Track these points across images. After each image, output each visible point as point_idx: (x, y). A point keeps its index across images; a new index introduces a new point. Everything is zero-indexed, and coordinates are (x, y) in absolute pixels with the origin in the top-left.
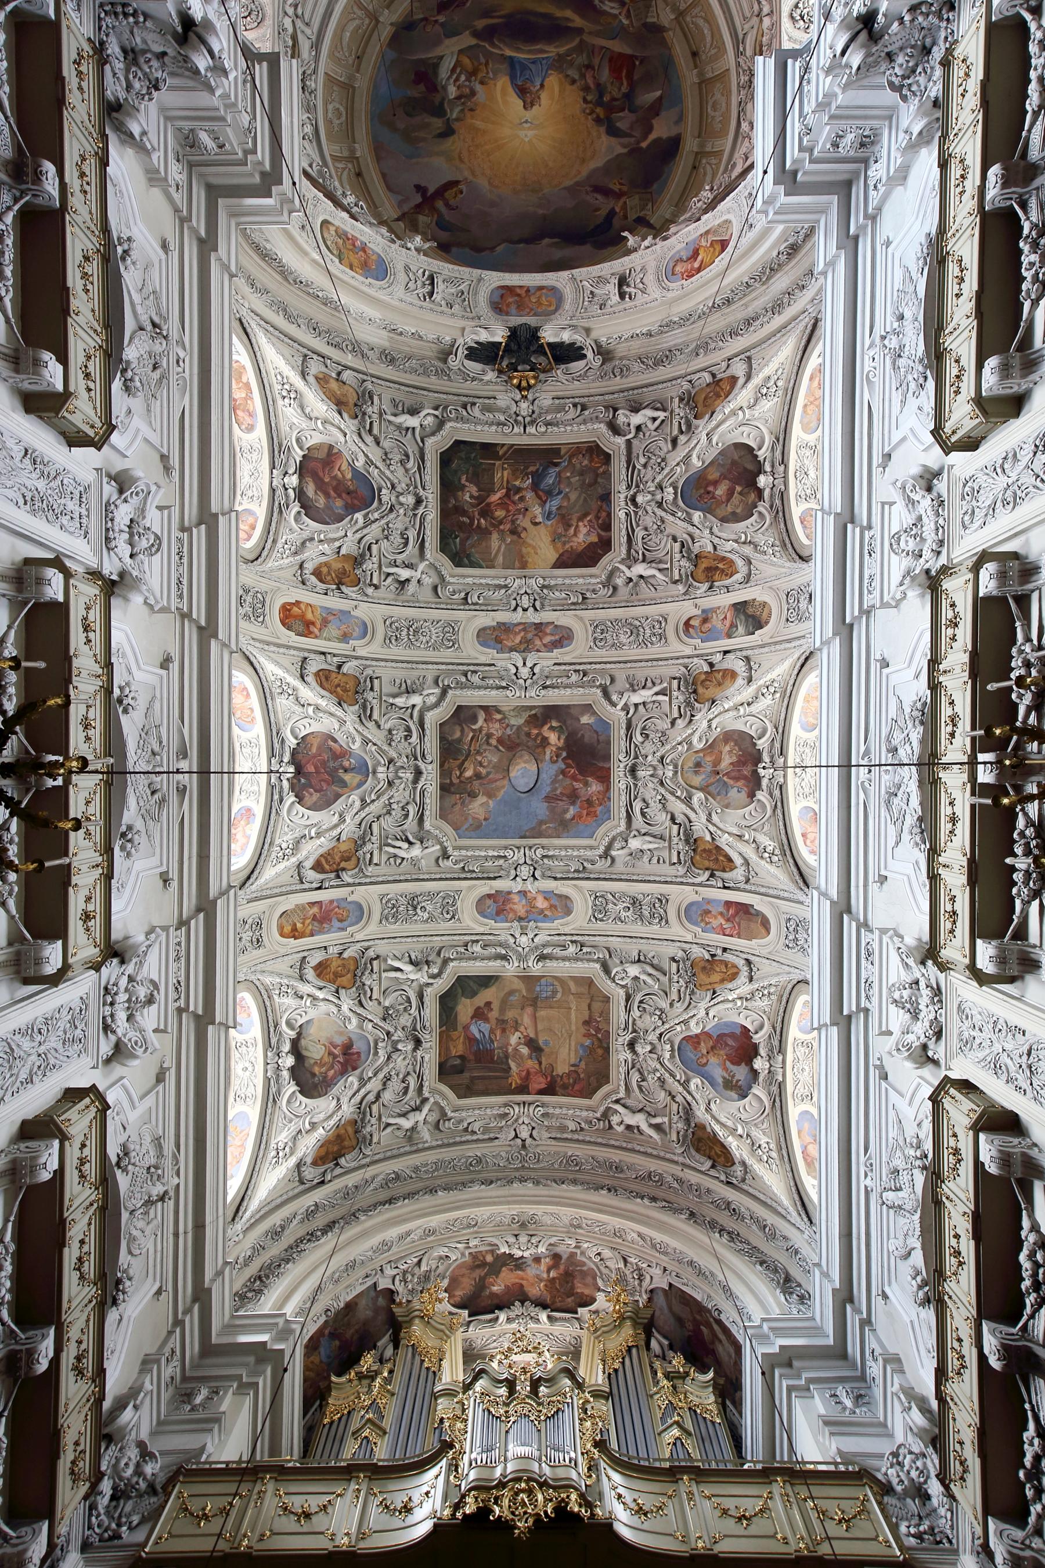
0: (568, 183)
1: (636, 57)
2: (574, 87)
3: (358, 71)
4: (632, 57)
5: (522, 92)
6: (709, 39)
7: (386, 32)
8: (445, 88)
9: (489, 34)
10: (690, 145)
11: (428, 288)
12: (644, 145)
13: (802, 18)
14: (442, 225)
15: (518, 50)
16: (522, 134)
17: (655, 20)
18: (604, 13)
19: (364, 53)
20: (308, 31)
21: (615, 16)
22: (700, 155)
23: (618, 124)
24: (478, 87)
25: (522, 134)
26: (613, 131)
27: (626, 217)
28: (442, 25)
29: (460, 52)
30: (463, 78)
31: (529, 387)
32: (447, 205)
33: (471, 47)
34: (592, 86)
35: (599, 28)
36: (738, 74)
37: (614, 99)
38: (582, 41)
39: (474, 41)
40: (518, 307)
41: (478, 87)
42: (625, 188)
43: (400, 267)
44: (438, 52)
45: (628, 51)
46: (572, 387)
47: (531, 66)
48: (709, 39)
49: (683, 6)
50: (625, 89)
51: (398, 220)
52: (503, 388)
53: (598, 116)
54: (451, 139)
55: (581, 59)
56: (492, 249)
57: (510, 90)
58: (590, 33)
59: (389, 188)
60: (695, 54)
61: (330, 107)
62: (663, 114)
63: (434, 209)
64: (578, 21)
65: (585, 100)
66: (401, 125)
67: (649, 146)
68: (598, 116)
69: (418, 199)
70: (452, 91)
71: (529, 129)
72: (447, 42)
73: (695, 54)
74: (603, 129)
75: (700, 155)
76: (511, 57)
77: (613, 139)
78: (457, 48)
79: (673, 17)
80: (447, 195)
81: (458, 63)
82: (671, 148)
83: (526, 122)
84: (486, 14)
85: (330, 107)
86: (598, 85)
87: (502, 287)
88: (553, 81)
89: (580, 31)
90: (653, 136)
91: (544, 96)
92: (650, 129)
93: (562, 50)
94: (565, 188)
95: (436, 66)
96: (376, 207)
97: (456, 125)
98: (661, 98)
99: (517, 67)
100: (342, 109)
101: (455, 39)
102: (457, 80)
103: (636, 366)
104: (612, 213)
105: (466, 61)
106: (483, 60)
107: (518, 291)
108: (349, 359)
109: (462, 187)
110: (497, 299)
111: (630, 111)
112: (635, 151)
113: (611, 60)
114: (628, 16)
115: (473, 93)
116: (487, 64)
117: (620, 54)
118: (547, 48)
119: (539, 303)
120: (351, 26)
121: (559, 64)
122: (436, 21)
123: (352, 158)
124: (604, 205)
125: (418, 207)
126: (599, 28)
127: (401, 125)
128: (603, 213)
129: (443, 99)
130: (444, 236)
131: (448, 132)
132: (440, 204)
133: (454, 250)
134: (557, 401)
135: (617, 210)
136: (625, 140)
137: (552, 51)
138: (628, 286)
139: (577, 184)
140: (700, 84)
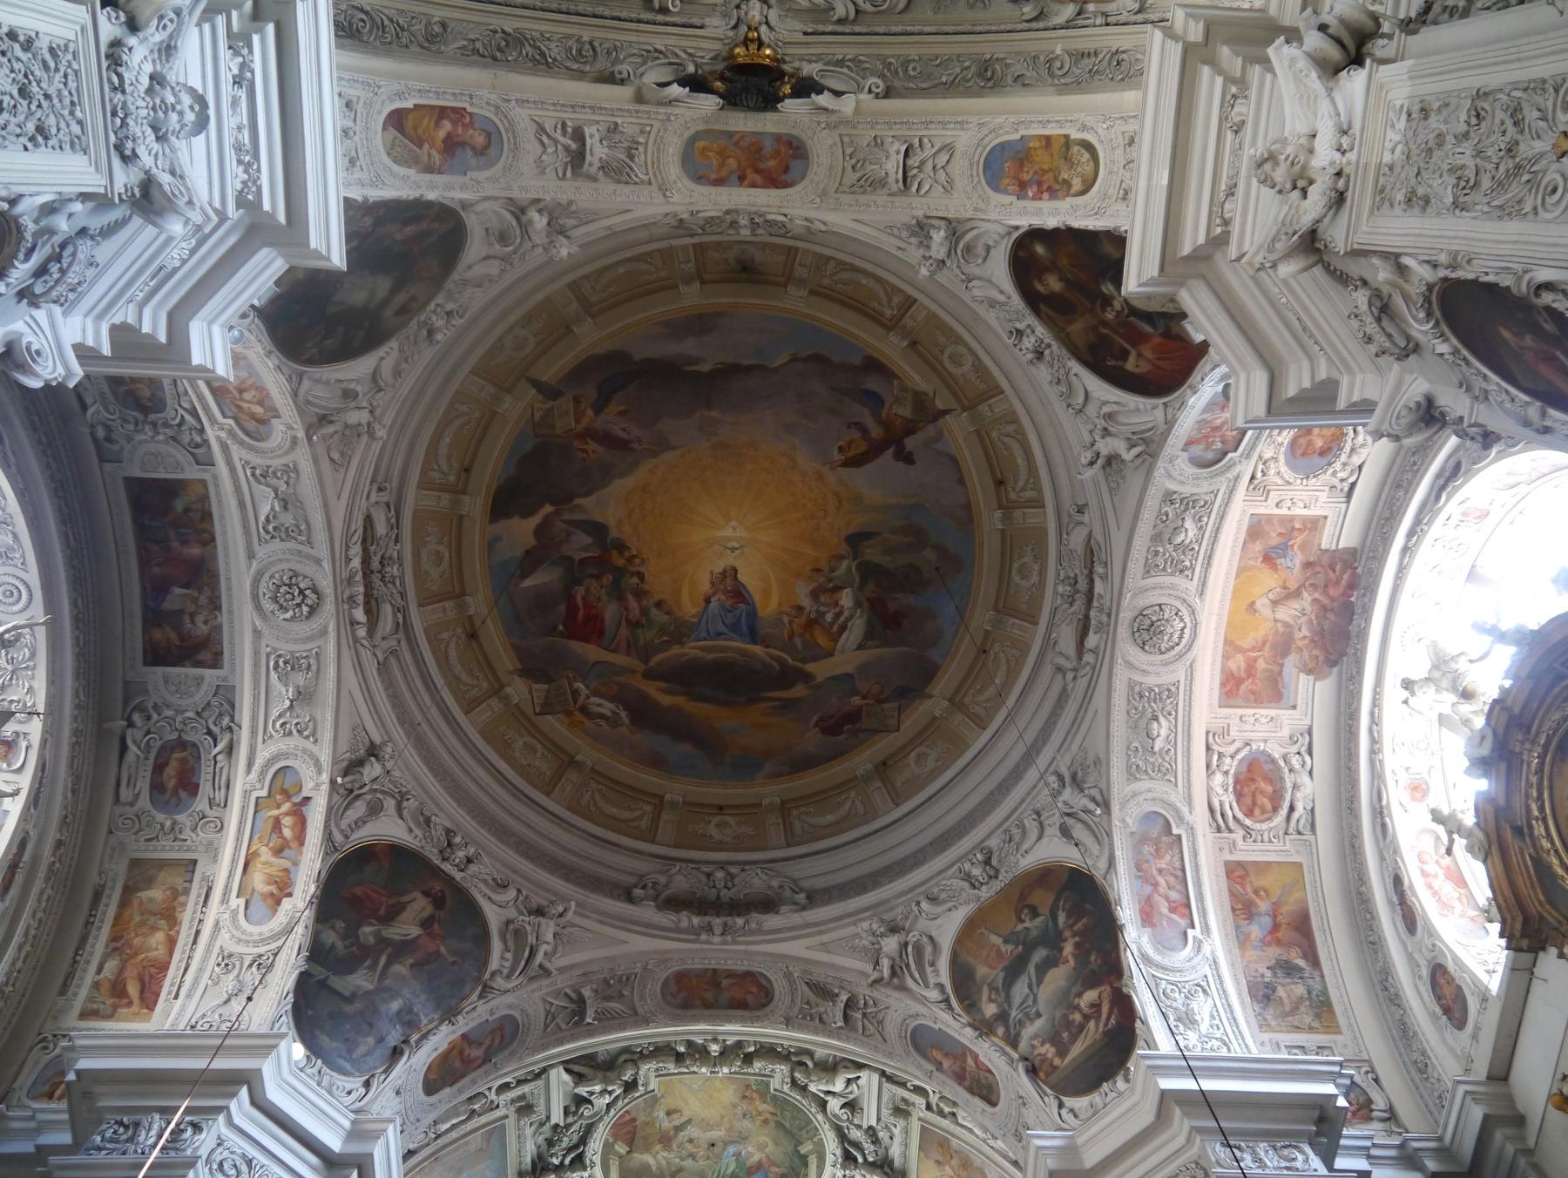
0: (669, 457)
1: (562, 635)
2: (657, 597)
3: (987, 633)
4: (570, 637)
5: (739, 594)
6: (453, 653)
7: (942, 686)
8: (858, 604)
9: (788, 676)
10: (476, 505)
11: (910, 162)
12: (548, 509)
13: (301, 592)
14: (874, 400)
15: (743, 652)
16: (741, 533)
17: (535, 686)
18: (612, 699)
19: (976, 659)
20: (1061, 661)
21: (596, 693)
22: (458, 490)
23: (588, 540)
24: (806, 602)
25: (741, 533)
26: (598, 530)
27: (576, 400)
28: (855, 692)
29: (830, 654)
30: (829, 617)
31: (746, 42)
32: (865, 431)
33: (815, 659)
34: (630, 597)
35: (619, 679)
36: (402, 578)
37: (597, 577)
38: (646, 662)
39: (809, 667)
40: (760, 149)
41: (806, 602)
42: (577, 444)
43: (960, 184)
44: (865, 655)
45: (578, 647)
46: (672, 41)
47: (723, 629)
48: (453, 653)
49: (495, 703)
50: (580, 592)
51: (945, 412)
52: (791, 50)
53: (621, 553)
54: (852, 530)
55: (646, 636)
56: (795, 359)
57: (757, 598)
58: (634, 672)
59: (954, 461)
60: (473, 636)
61: (1035, 579)
62: (519, 553)
63: (886, 425)
64: (653, 689)
65: (641, 576)
66: (929, 554)
67: (541, 506)
68: (621, 553)
69: (910, 443)
70: (846, 599)
71: (729, 539)
72: (850, 668)
73: (473, 636)
74: (614, 533)
75: (458, 490)
76: (755, 642)
77: (600, 519)
78: (837, 658)
79: (509, 690)
80: (862, 447)
81: (835, 638)
82: (506, 503)
83: (733, 550)
84: (788, 705)
85: (1035, 579)
86: (621, 598)
87: (786, 185)
88: (689, 608)
89: (649, 675)
90: (535, 521)
91: (705, 585)
92: (539, 531)
93: (676, 650)
94: (674, 448)
95: (869, 635)
96: (978, 432)
97: (844, 549)
98: (524, 576)
99: (745, 629)
100: (1017, 579)
101: (837, 672)
102: (838, 615)
103: (554, 50)
104: (599, 408)
105: (822, 640)
106: (798, 641)
107: (758, 178)
108: (1059, 45)
109: (837, 457)
110: (796, 165)
111: (570, 559)
112: (563, 499)
113: (601, 633)
114: (575, 693)
115: (814, 594)
116: (791, 636)
117: (586, 640)
118: (700, 654)
119: (723, 155)
120: (991, 691)
121: (680, 632)
122: (864, 697)
123: (1007, 507)
124: (612, 421)
125: (911, 431)
126: (619, 679)
127: (929, 554)
128: (614, 407)
129: (861, 588)
130: (873, 383)
131: (856, 540)
132: (876, 432)
133: (857, 361)
134: (696, 21)
135: (590, 412)
136: (577, 516)
137: (691, 649)
138: (567, 148)
139: (655, 454)
140: (463, 594)
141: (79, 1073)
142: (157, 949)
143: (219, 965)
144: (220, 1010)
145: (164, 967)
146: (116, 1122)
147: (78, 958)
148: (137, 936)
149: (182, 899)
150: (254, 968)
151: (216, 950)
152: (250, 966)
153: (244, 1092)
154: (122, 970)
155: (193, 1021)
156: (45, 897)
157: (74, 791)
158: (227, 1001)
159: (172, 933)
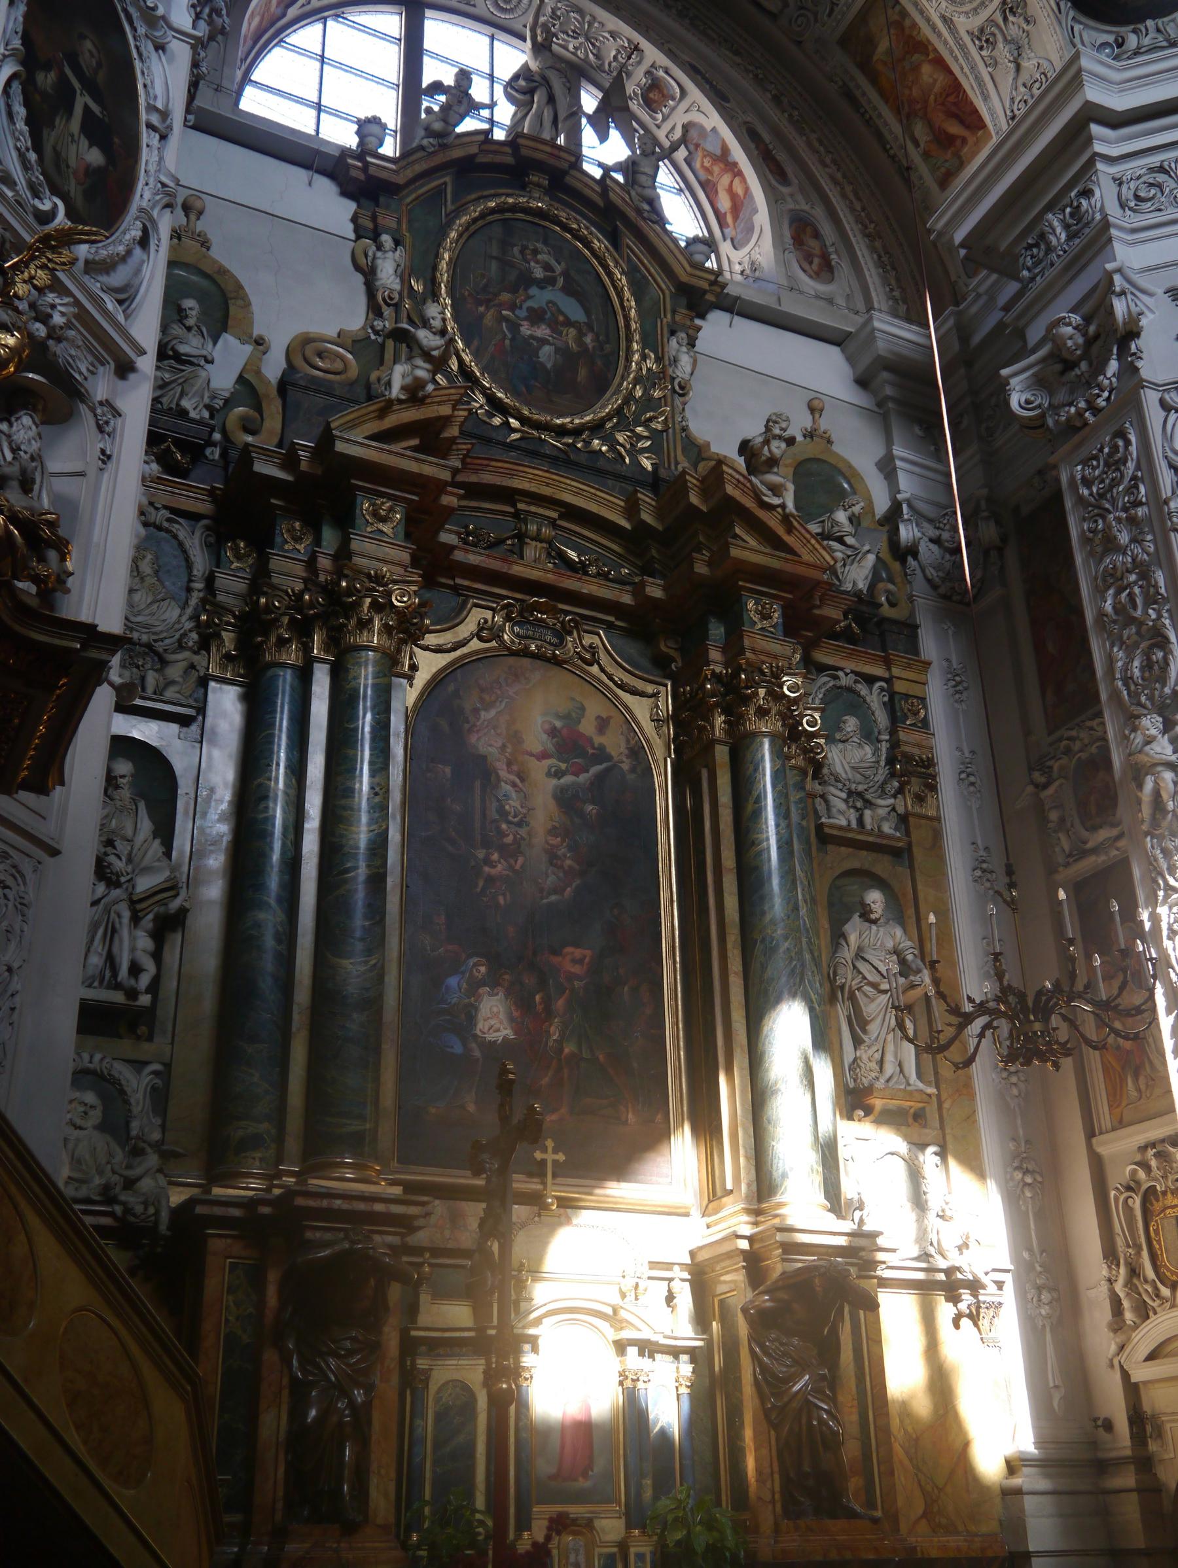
141: (963, 245)
142: (935, 81)
143: (981, 48)
144: (1020, 82)
145: (956, 86)
146: (1026, 249)
147: (892, 152)
148: (910, 89)
149: (907, 23)
150: (1011, 18)
151: (967, 39)
152: (1005, 19)
153: (1095, 129)
154: (930, 124)
155: (1008, 113)
156: (816, 144)
157: (737, 53)
158: (1018, 68)
159: (931, 56)
